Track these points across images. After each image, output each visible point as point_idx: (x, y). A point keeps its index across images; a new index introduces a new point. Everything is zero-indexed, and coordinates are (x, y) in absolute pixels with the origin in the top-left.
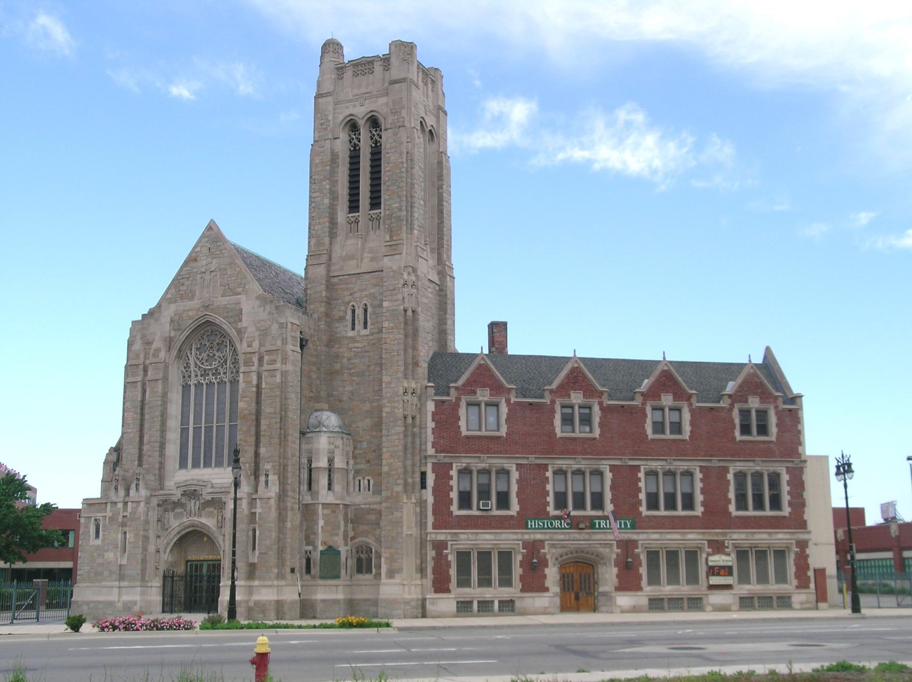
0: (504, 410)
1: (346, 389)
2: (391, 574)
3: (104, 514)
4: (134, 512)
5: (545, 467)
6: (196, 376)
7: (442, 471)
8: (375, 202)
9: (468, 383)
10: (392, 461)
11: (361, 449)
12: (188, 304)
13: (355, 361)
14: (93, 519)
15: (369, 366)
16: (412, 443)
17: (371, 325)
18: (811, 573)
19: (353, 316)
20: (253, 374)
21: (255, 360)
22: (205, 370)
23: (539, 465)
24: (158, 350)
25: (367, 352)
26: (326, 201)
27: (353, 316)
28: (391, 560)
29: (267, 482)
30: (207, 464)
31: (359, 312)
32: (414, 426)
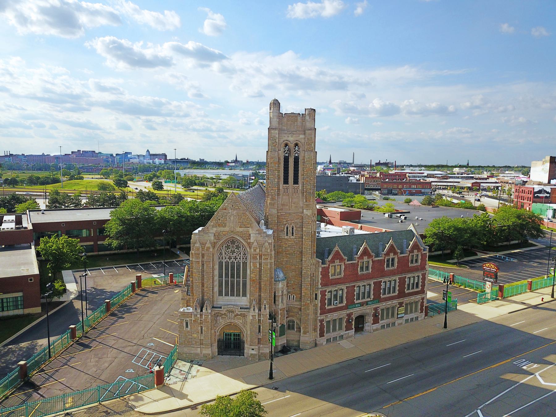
0: (343, 267)
1: (284, 259)
2: (305, 333)
3: (191, 319)
4: (205, 319)
5: (354, 286)
6: (226, 258)
7: (323, 294)
8: (296, 182)
9: (332, 258)
10: (306, 291)
11: (290, 284)
12: (222, 229)
13: (288, 249)
14: (184, 320)
15: (294, 251)
16: (313, 284)
17: (295, 235)
18: (424, 308)
19: (287, 230)
20: (257, 263)
21: (258, 257)
22: (230, 256)
23: (353, 286)
24: (209, 248)
25: (293, 245)
26: (276, 180)
27: (287, 230)
28: (305, 328)
29: (265, 308)
30: (232, 295)
31: (290, 229)
32: (313, 276)
